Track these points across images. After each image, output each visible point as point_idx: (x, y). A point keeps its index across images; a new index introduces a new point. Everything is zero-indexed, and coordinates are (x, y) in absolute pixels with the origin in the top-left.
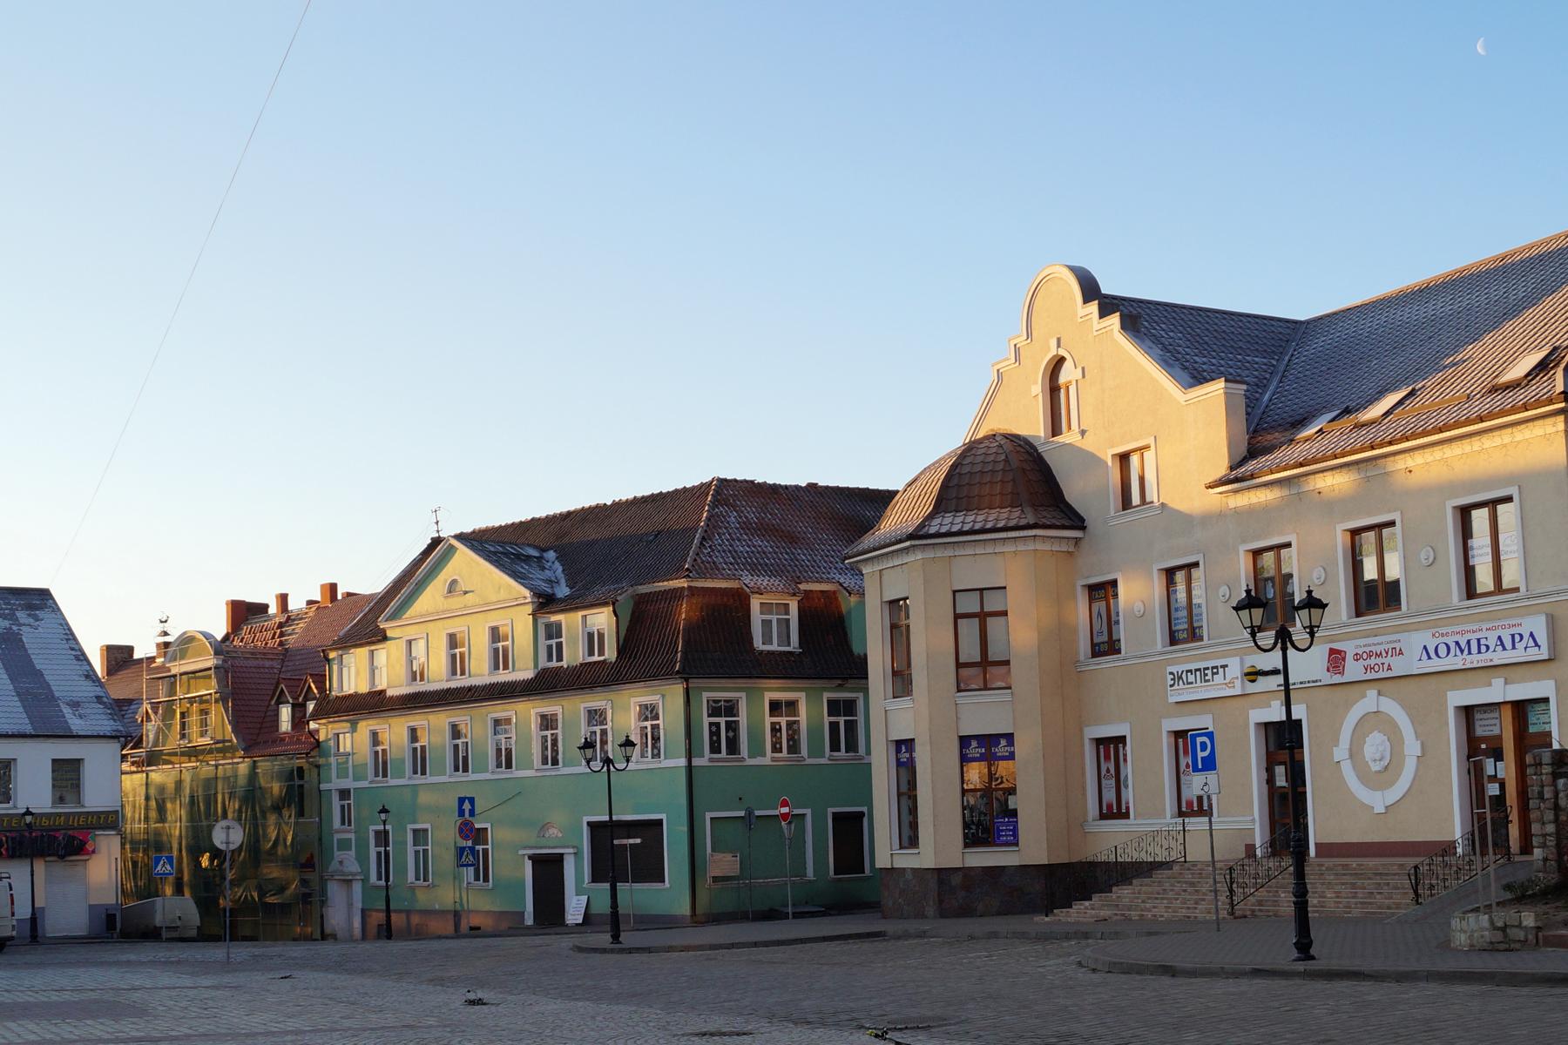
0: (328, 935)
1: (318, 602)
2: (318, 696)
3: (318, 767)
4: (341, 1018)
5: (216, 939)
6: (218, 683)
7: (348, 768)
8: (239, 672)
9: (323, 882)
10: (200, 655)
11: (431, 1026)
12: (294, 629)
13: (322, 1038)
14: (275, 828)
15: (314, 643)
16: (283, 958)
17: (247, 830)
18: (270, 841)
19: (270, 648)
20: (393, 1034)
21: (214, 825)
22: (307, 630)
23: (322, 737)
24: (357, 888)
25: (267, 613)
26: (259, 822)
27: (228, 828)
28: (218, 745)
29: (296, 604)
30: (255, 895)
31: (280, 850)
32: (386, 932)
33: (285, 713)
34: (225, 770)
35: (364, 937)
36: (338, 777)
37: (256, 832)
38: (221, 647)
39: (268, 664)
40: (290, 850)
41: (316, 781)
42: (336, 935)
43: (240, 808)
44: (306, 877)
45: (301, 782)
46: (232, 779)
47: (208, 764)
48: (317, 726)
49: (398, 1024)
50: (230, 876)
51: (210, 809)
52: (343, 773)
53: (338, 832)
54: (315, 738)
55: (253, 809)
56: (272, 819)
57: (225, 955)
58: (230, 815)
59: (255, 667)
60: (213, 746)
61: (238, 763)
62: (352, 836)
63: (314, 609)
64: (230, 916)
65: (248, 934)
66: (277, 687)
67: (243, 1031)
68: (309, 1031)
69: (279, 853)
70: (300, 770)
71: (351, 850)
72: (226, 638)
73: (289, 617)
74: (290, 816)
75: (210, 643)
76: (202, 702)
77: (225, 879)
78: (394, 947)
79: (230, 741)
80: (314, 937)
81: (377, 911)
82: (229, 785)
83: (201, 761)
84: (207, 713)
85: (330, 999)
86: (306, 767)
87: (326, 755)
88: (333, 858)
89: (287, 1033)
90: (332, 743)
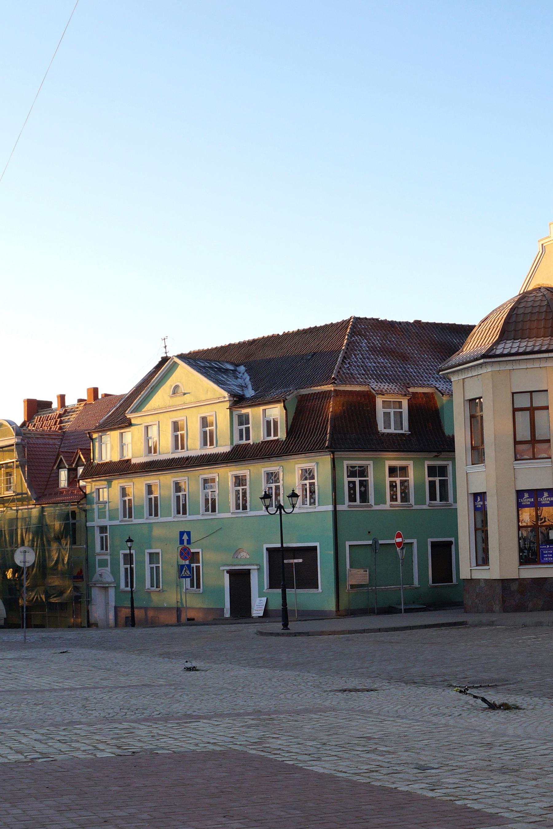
0: (93, 624)
1: (85, 400)
2: (85, 463)
3: (85, 511)
4: (101, 679)
5: (17, 626)
6: (18, 454)
7: (105, 512)
8: (33, 447)
9: (89, 588)
10: (6, 436)
11: (161, 685)
12: (69, 419)
13: (88, 693)
14: (57, 552)
15: (82, 428)
16: (62, 639)
17: (38, 554)
18: (53, 561)
19: (53, 431)
20: (136, 690)
21: (16, 550)
22: (77, 419)
23: (88, 491)
24: (112, 592)
25: (51, 407)
26: (46, 548)
27: (25, 552)
28: (18, 497)
29: (70, 402)
30: (43, 597)
31: (60, 567)
32: (131, 622)
33: (63, 475)
34: (23, 513)
35: (116, 625)
36: (99, 518)
37: (44, 556)
38: (20, 431)
39: (51, 442)
40: (66, 567)
41: (84, 520)
42: (97, 624)
43: (33, 538)
44: (77, 585)
45: (74, 521)
46: (27, 519)
47: (12, 509)
48: (85, 483)
49: (139, 684)
50: (26, 584)
51: (13, 539)
52: (102, 515)
53: (99, 554)
54: (83, 492)
55: (42, 540)
56: (54, 546)
57: (23, 637)
58: (26, 543)
59: (43, 444)
60: (15, 497)
61: (31, 508)
62: (108, 557)
63: (82, 405)
64: (27, 611)
65: (37, 624)
66: (57, 458)
67: (35, 689)
68: (80, 688)
69: (59, 568)
70: (74, 513)
71: (107, 567)
72: (24, 424)
73: (66, 410)
74: (67, 544)
75: (13, 428)
76: (7, 467)
77: (23, 586)
78: (137, 632)
79: (26, 493)
80: (82, 625)
81: (126, 607)
82: (25, 523)
83: (7, 507)
84: (11, 475)
85: (94, 667)
86: (77, 511)
87: (91, 502)
88: (95, 572)
89: (64, 689)
90: (95, 495)
